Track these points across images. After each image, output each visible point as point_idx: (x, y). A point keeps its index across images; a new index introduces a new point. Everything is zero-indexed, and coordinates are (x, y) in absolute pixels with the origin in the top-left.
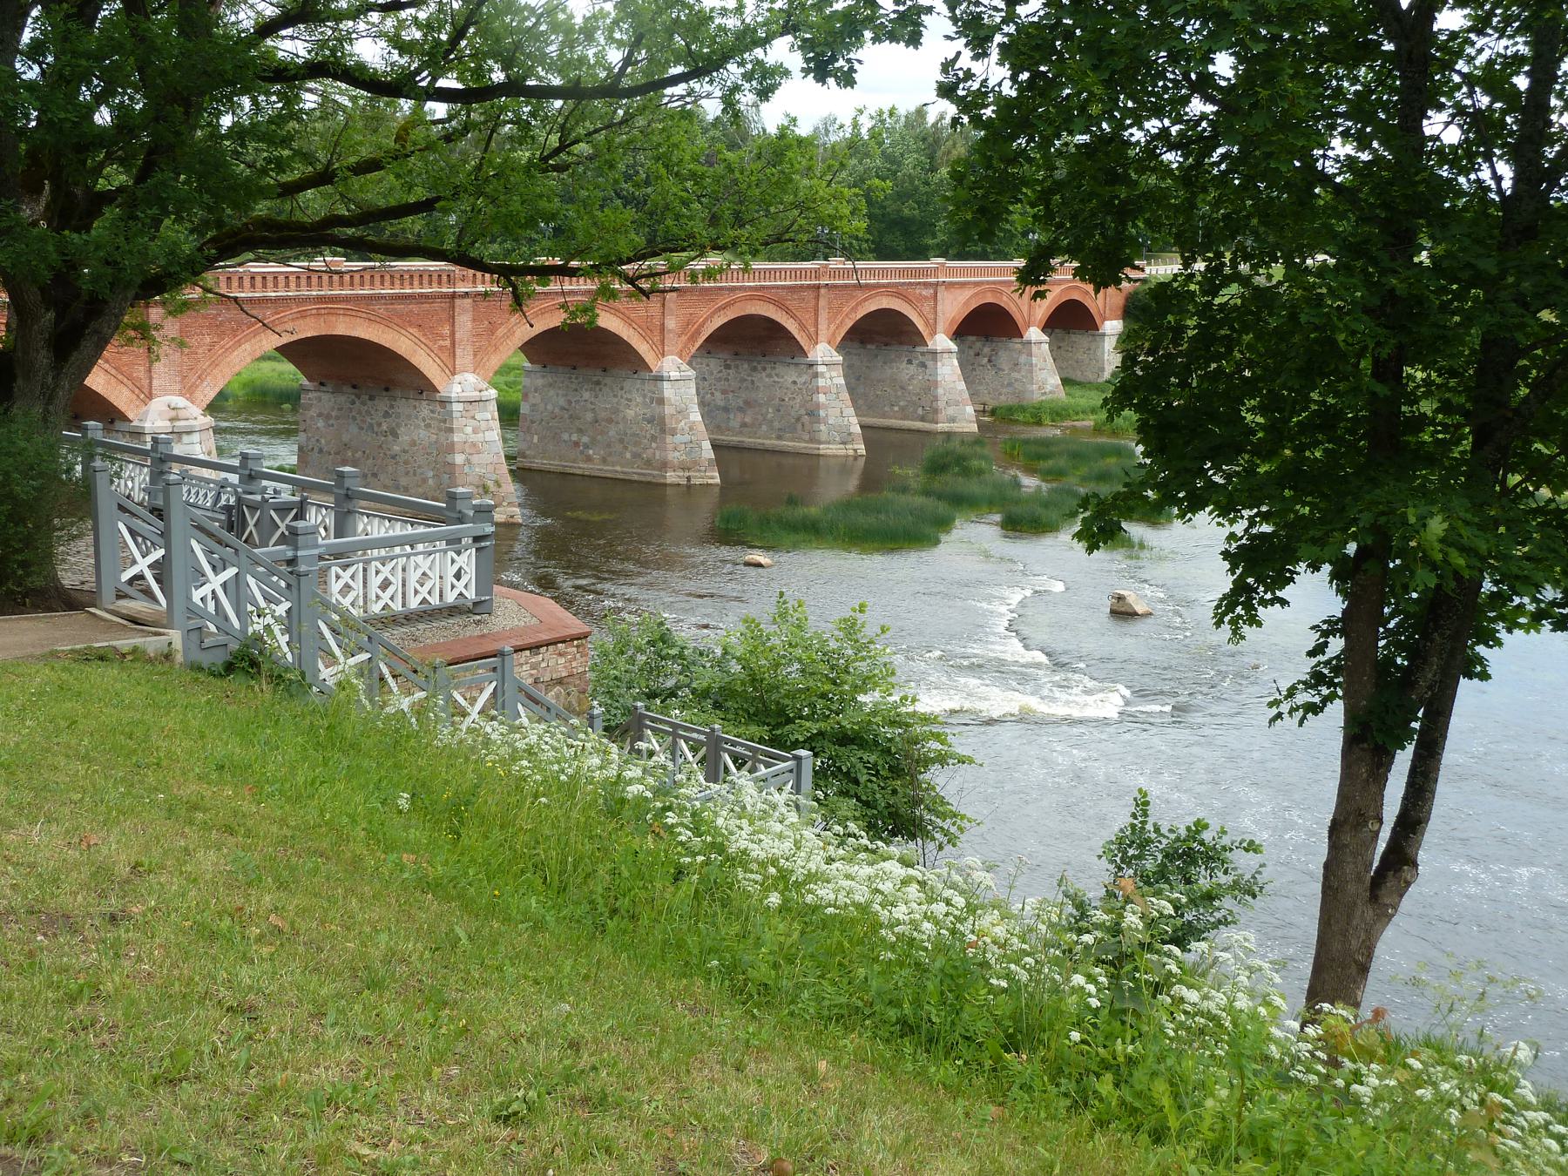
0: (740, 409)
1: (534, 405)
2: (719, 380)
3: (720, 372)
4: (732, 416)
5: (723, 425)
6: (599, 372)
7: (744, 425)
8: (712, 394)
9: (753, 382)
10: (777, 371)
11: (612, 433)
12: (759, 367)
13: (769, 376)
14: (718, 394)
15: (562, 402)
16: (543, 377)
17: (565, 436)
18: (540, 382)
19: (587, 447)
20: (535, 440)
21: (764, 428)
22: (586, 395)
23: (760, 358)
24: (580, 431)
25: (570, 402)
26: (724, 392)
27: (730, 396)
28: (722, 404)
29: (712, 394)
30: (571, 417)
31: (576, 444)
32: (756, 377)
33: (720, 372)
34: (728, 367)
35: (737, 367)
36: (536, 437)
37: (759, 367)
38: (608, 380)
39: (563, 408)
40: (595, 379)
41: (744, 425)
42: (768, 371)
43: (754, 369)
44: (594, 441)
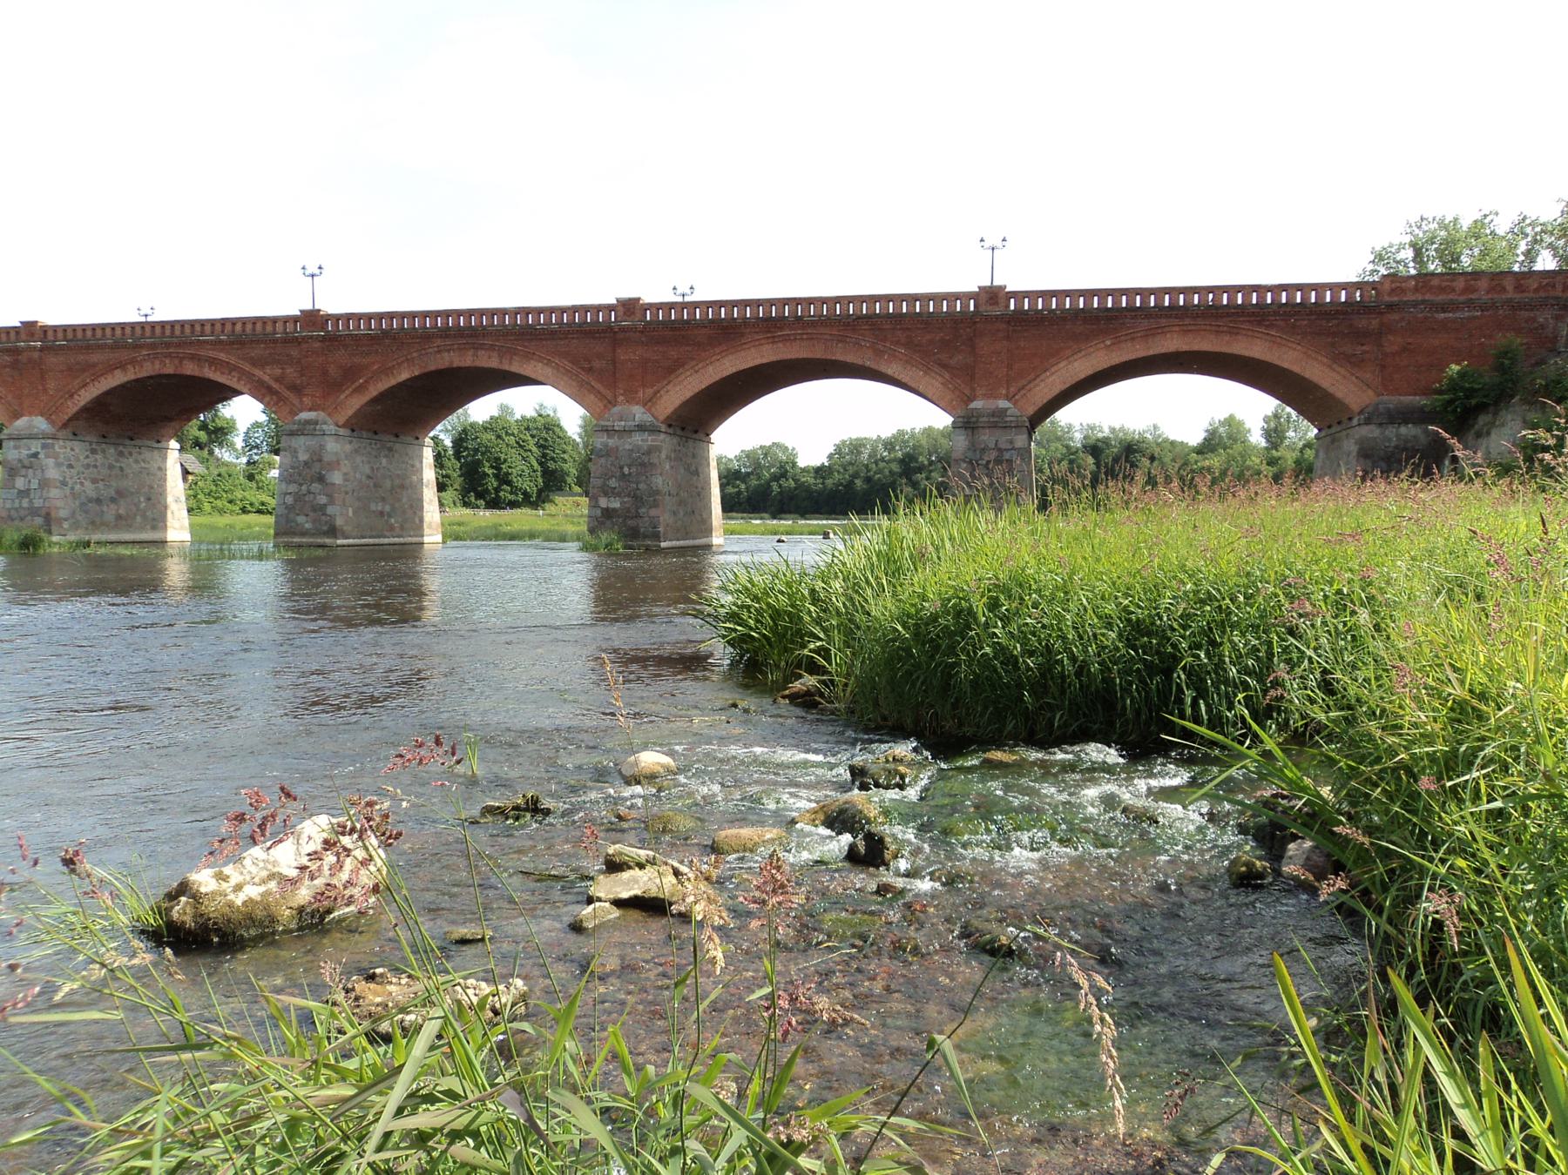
0: (113, 500)
1: (345, 474)
2: (88, 466)
3: (87, 457)
4: (105, 508)
5: (98, 520)
6: (394, 439)
7: (119, 517)
8: (82, 484)
9: (121, 469)
10: (142, 457)
11: (404, 500)
12: (126, 451)
13: (137, 461)
14: (87, 483)
15: (367, 470)
16: (350, 442)
17: (373, 507)
18: (348, 448)
19: (390, 516)
20: (351, 514)
21: (139, 519)
22: (384, 461)
23: (128, 442)
24: (383, 499)
25: (372, 468)
26: (94, 481)
27: (101, 485)
28: (93, 495)
29: (82, 484)
30: (376, 485)
31: (382, 513)
32: (124, 462)
33: (87, 457)
34: (94, 451)
35: (103, 451)
36: (350, 510)
37: (126, 451)
38: (398, 446)
39: (369, 477)
40: (389, 445)
41: (119, 517)
42: (135, 455)
43: (121, 454)
44: (393, 508)
